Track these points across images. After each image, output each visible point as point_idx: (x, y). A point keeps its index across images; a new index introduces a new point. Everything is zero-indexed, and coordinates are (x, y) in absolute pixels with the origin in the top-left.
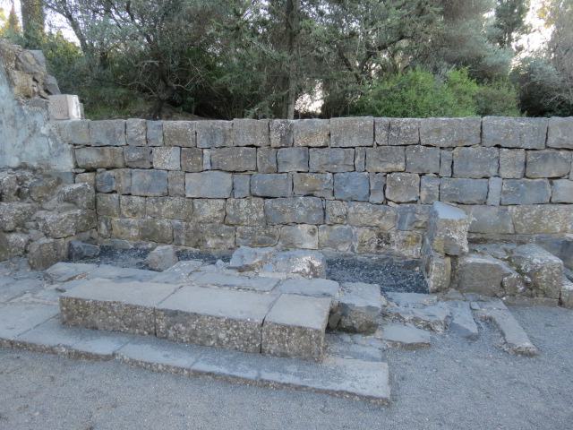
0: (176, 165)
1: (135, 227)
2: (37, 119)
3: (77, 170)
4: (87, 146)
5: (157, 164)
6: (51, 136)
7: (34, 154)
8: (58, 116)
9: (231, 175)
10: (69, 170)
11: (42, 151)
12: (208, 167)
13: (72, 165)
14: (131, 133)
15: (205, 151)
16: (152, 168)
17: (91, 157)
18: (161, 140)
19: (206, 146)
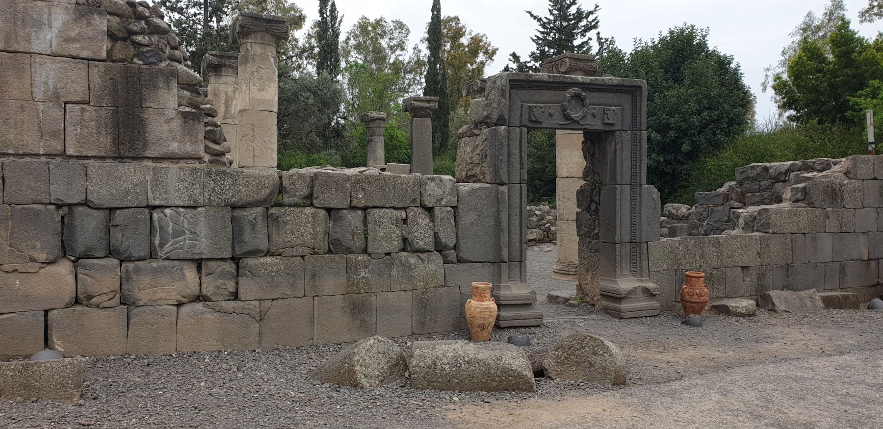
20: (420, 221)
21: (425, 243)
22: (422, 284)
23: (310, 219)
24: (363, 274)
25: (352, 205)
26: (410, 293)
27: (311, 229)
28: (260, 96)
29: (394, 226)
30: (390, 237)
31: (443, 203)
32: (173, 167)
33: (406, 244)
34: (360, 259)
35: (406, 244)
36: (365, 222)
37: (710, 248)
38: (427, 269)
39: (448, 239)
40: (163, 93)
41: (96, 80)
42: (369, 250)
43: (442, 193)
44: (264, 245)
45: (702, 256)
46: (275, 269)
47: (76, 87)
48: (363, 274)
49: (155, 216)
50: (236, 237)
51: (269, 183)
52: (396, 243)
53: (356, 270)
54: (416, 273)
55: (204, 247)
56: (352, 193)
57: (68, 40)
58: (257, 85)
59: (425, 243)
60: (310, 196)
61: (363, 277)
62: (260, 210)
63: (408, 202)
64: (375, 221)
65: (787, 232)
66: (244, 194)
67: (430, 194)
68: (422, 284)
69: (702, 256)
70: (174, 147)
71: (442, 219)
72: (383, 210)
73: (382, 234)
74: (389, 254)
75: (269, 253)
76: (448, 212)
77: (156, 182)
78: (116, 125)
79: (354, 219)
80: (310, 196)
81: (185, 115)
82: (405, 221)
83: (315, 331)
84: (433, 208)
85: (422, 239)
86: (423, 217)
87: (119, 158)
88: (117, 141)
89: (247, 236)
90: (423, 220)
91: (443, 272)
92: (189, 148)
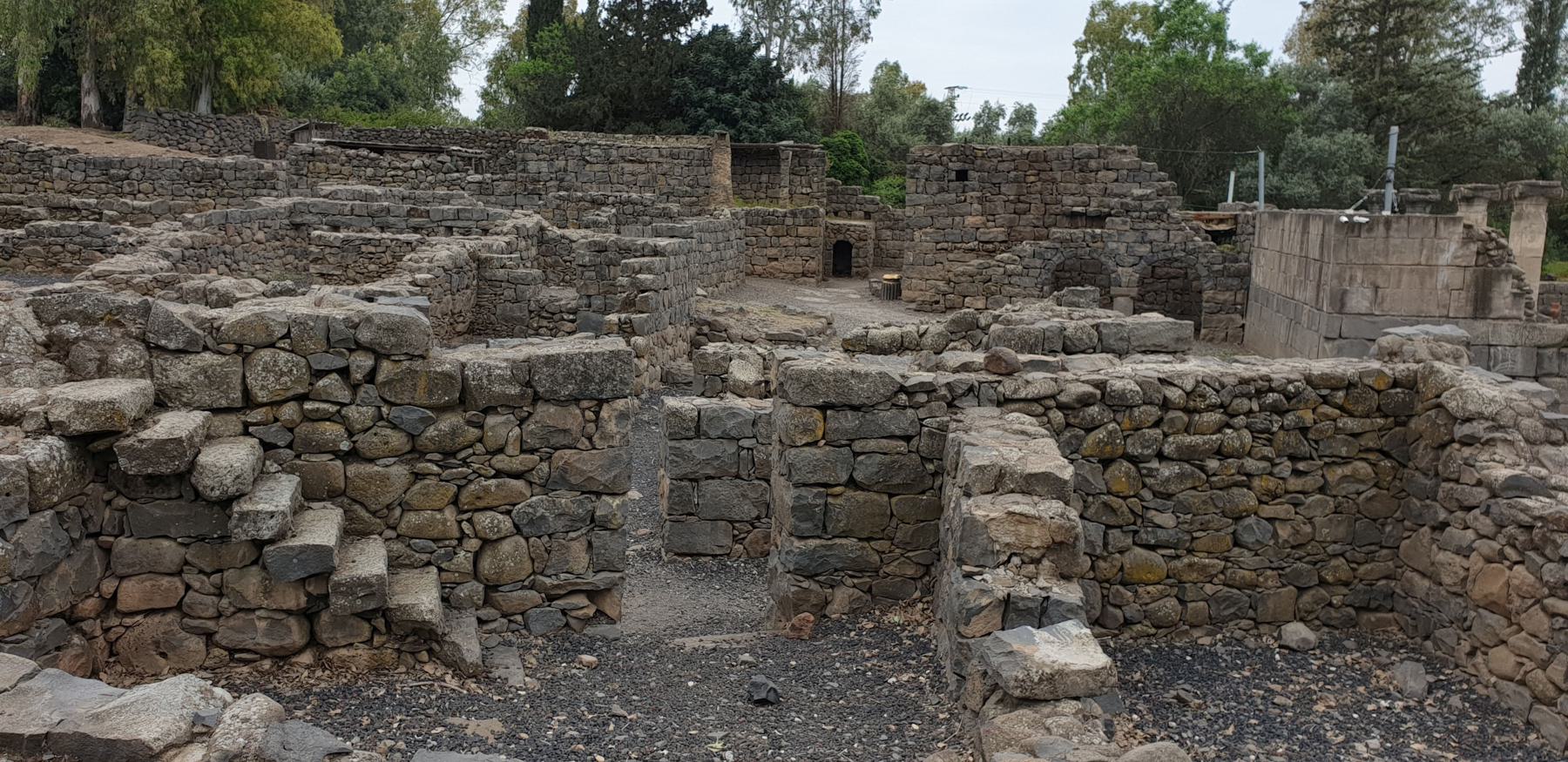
28: (1529, 245)
32: (1505, 323)
40: (1503, 283)
41: (1468, 277)
44: (1556, 370)
47: (1458, 282)
49: (1492, 350)
50: (1539, 364)
55: (1519, 369)
57: (1456, 258)
62: (1555, 350)
66: (1547, 340)
70: (1507, 312)
75: (1558, 375)
77: (1494, 332)
78: (1476, 300)
81: (1515, 295)
87: (1475, 318)
88: (1476, 310)
89: (1546, 365)
92: (1515, 313)
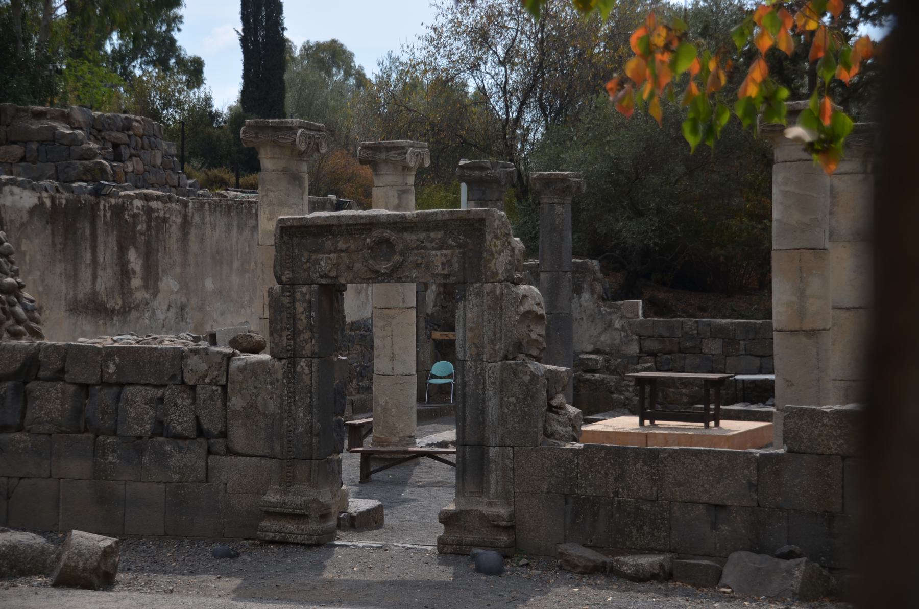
0: (719, 351)
1: (686, 395)
2: (613, 318)
3: (641, 355)
4: (650, 337)
5: (706, 351)
6: (623, 329)
7: (608, 342)
8: (629, 315)
9: (759, 358)
10: (635, 354)
11: (615, 340)
12: (743, 352)
13: (638, 351)
14: (687, 328)
15: (741, 342)
16: (701, 353)
17: (653, 345)
18: (709, 334)
19: (742, 338)
20: (179, 401)
21: (184, 429)
22: (177, 477)
23: (59, 395)
24: (110, 458)
25: (103, 381)
26: (162, 486)
27: (59, 406)
29: (147, 407)
30: (143, 419)
31: (207, 380)
33: (161, 428)
34: (108, 441)
35: (161, 428)
36: (118, 399)
37: (639, 466)
38: (185, 460)
39: (212, 425)
42: (119, 432)
43: (207, 368)
45: (620, 478)
46: (22, 445)
48: (110, 458)
51: (20, 357)
52: (148, 426)
53: (104, 454)
54: (173, 462)
56: (103, 367)
58: (267, 212)
59: (184, 429)
60: (62, 371)
61: (111, 463)
63: (166, 379)
64: (127, 399)
65: (828, 452)
67: (192, 370)
68: (177, 477)
69: (620, 478)
71: (205, 400)
72: (138, 387)
73: (133, 415)
74: (140, 438)
75: (20, 429)
76: (213, 391)
79: (105, 396)
80: (62, 371)
82: (161, 400)
83: (61, 517)
84: (193, 388)
85: (180, 423)
86: (185, 396)
90: (184, 401)
91: (204, 464)
